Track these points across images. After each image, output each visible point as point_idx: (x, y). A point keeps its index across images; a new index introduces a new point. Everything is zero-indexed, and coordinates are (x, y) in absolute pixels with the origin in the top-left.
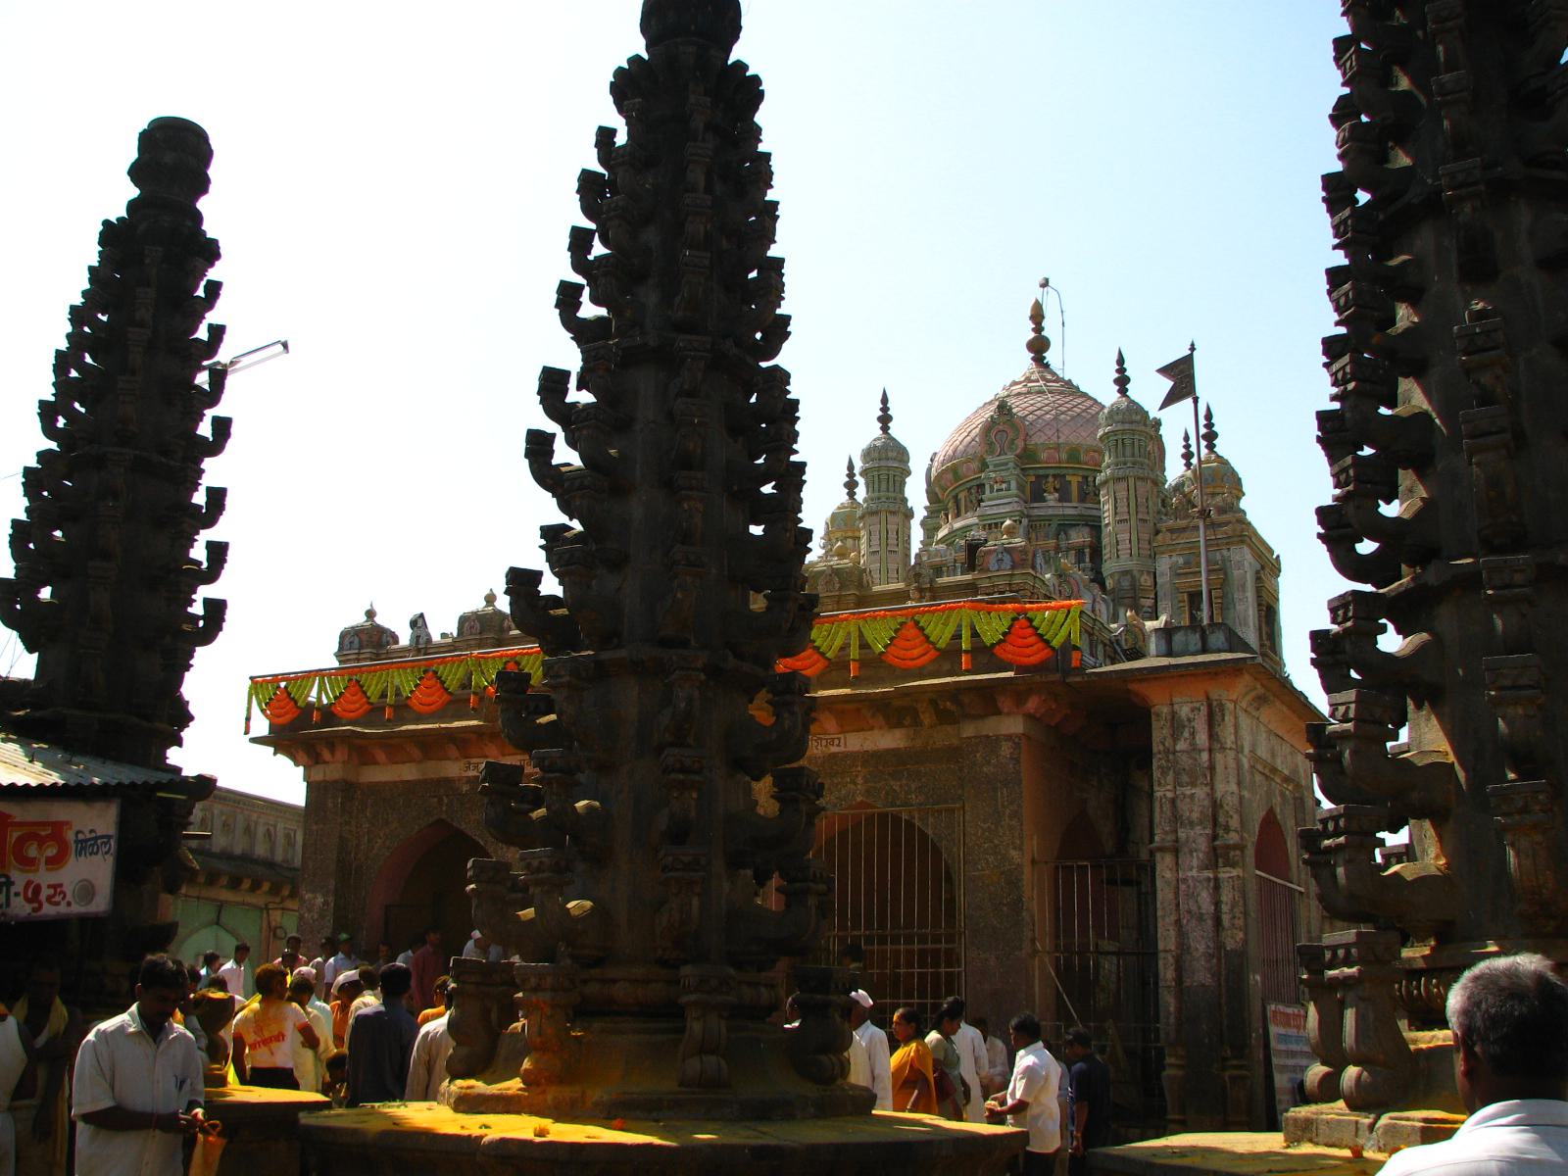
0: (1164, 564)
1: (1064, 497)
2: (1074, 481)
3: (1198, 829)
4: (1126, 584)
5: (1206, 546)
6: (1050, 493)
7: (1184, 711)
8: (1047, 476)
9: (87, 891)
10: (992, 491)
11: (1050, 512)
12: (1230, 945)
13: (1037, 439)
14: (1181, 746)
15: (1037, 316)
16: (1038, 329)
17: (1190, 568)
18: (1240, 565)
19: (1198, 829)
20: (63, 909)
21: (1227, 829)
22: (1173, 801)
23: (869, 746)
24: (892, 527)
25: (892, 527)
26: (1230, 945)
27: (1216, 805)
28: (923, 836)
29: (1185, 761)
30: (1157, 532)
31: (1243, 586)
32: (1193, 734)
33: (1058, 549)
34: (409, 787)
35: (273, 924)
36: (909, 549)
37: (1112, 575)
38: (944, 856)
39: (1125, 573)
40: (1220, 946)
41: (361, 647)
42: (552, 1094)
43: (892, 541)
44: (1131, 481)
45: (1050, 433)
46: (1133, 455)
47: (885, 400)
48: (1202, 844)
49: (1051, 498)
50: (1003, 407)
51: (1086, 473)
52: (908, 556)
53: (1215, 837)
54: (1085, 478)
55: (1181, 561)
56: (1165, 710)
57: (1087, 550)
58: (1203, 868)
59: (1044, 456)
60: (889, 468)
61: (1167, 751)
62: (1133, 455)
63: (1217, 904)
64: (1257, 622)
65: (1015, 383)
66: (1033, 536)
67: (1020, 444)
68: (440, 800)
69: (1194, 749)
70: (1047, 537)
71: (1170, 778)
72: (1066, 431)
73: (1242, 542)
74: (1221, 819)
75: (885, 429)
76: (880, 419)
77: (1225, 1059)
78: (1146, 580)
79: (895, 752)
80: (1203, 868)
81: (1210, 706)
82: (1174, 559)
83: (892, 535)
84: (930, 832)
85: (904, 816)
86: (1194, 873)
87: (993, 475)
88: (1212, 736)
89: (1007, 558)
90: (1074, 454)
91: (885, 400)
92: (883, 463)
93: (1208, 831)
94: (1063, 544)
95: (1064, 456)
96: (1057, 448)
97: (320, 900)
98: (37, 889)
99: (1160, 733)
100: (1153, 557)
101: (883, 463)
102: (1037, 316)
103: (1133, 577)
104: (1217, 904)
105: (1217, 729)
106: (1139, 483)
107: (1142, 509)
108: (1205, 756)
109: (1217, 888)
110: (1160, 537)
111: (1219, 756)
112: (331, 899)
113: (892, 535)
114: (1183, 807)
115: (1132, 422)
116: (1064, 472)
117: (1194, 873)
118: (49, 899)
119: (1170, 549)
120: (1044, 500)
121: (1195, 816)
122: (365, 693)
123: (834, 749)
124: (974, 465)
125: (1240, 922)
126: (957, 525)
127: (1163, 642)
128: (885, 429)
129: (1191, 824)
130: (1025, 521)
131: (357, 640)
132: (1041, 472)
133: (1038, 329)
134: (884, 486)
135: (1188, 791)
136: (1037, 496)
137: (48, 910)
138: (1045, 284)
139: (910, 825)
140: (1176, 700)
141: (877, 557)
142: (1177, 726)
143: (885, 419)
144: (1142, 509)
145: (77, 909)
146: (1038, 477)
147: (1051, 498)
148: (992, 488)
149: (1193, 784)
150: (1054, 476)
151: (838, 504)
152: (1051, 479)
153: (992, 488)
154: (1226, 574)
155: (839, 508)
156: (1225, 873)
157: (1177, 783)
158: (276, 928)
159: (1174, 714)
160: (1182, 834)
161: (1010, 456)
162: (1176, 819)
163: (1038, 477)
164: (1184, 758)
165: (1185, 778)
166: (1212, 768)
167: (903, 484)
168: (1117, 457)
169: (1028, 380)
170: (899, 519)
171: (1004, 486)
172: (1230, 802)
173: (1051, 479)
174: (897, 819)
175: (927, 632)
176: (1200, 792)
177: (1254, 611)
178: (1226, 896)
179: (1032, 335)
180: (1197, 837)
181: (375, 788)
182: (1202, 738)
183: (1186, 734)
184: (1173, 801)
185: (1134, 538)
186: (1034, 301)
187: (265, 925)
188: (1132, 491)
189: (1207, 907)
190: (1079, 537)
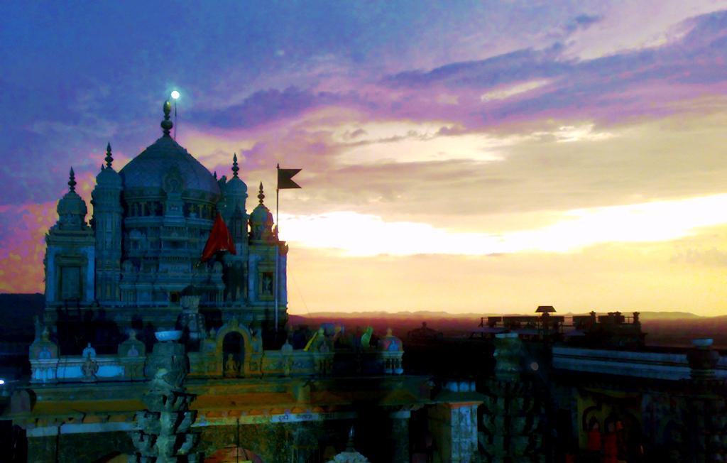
3: (467, 454)
8: (191, 204)
14: (462, 424)
19: (467, 454)
32: (466, 420)
56: (457, 411)
69: (466, 425)
71: (458, 436)
100: (248, 254)
121: (467, 449)
142: (461, 417)
147: (193, 215)
149: (466, 438)
150: (194, 204)
159: (460, 413)
160: (462, 455)
166: (472, 432)
183: (464, 420)
184: (459, 443)
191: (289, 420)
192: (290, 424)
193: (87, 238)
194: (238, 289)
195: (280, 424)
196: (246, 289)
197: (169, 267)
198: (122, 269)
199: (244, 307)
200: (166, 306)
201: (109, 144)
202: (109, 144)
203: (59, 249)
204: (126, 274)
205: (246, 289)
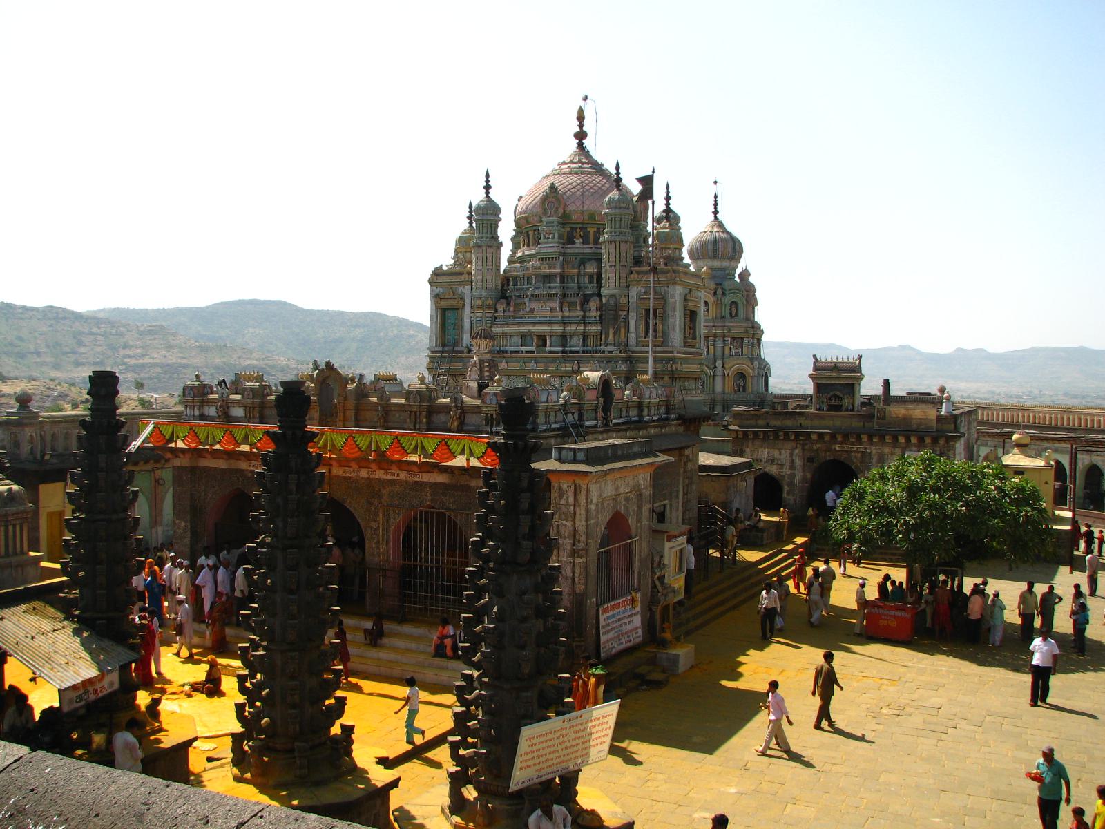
0: (634, 292)
1: (586, 241)
2: (592, 230)
4: (612, 302)
5: (654, 284)
6: (578, 239)
7: (565, 487)
9: (112, 684)
10: (544, 238)
11: (577, 251)
12: (578, 591)
13: (571, 208)
14: (562, 502)
15: (581, 117)
16: (581, 126)
17: (643, 297)
18: (673, 296)
20: (105, 692)
21: (579, 542)
22: (558, 526)
23: (432, 480)
24: (489, 255)
25: (489, 255)
26: (578, 591)
27: (575, 530)
28: (455, 524)
29: (564, 509)
30: (632, 273)
31: (674, 309)
32: (567, 498)
33: (579, 274)
34: (223, 471)
35: (157, 477)
36: (499, 266)
37: (605, 296)
38: (464, 533)
39: (612, 296)
40: (574, 590)
41: (194, 396)
42: (259, 780)
43: (489, 263)
44: (618, 244)
45: (578, 204)
46: (620, 228)
47: (487, 176)
48: (569, 547)
49: (578, 241)
50: (552, 188)
51: (599, 226)
52: (499, 270)
53: (574, 544)
54: (599, 229)
55: (643, 291)
57: (595, 276)
58: (569, 557)
59: (574, 217)
60: (488, 220)
61: (557, 504)
62: (620, 228)
63: (574, 573)
64: (683, 324)
65: (564, 163)
66: (566, 266)
67: (561, 211)
68: (238, 479)
69: (568, 504)
70: (573, 268)
72: (588, 203)
73: (675, 283)
74: (577, 537)
75: (487, 193)
76: (485, 187)
77: (574, 638)
78: (623, 301)
79: (443, 484)
80: (569, 557)
81: (575, 485)
82: (639, 289)
83: (489, 260)
84: (458, 522)
85: (447, 514)
86: (565, 559)
87: (545, 229)
88: (575, 499)
89: (494, 398)
90: (592, 217)
91: (487, 176)
92: (485, 217)
93: (572, 541)
94: (582, 272)
95: (586, 217)
96: (582, 213)
97: (183, 524)
98: (97, 691)
99: (554, 494)
100: (628, 287)
101: (485, 217)
102: (581, 117)
103: (616, 298)
104: (574, 573)
105: (578, 497)
106: (622, 244)
107: (622, 260)
108: (572, 508)
109: (574, 566)
110: (632, 276)
111: (578, 509)
112: (188, 524)
113: (489, 260)
114: (562, 530)
115: (620, 208)
116: (584, 226)
117: (565, 559)
118: (101, 692)
119: (638, 283)
120: (574, 243)
121: (566, 534)
122: (198, 437)
123: (417, 479)
124: (537, 219)
125: (583, 582)
126: (527, 252)
127: (557, 454)
128: (487, 193)
129: (565, 537)
130: (561, 258)
131: (192, 393)
132: (574, 226)
133: (581, 126)
134: (485, 230)
135: (564, 522)
136: (571, 241)
137: (100, 695)
138: (586, 98)
139: (450, 518)
140: (561, 481)
141: (481, 272)
142: (561, 493)
143: (487, 187)
144: (623, 260)
145: (109, 691)
146: (571, 228)
147: (578, 241)
148: (544, 236)
150: (581, 228)
151: (462, 230)
152: (578, 230)
153: (544, 236)
154: (665, 301)
155: (463, 233)
156: (578, 561)
157: (560, 519)
158: (159, 479)
161: (554, 219)
162: (558, 533)
163: (571, 228)
164: (563, 507)
165: (563, 517)
167: (497, 227)
168: (611, 228)
169: (571, 162)
170: (493, 250)
171: (551, 236)
172: (582, 529)
173: (578, 230)
174: (444, 514)
175: (451, 447)
176: (569, 524)
177: (680, 322)
178: (577, 571)
179: (578, 129)
180: (566, 543)
181: (207, 469)
182: (571, 500)
185: (618, 277)
186: (578, 108)
187: (153, 479)
188: (618, 250)
189: (569, 574)
190: (591, 268)
191: (377, 477)
192: (380, 480)
193: (463, 277)
194: (611, 331)
195: (368, 478)
196: (623, 330)
197: (534, 305)
198: (496, 311)
199: (616, 353)
200: (533, 352)
201: (618, 163)
202: (618, 163)
203: (440, 290)
204: (500, 314)
205: (623, 330)
